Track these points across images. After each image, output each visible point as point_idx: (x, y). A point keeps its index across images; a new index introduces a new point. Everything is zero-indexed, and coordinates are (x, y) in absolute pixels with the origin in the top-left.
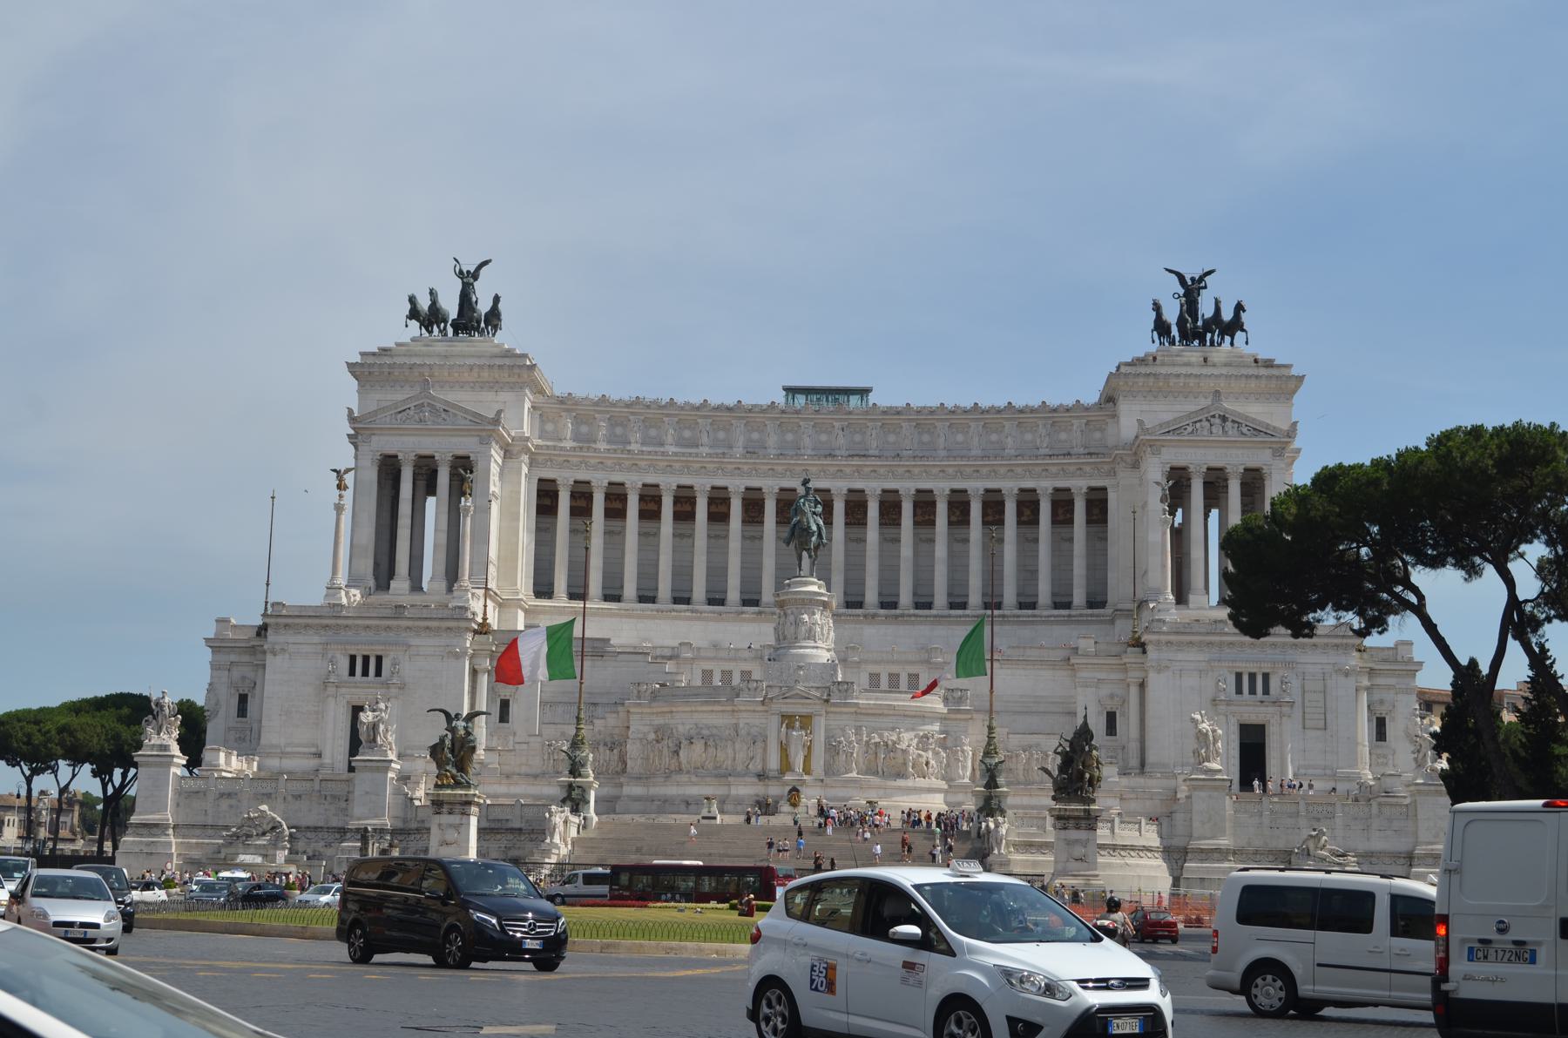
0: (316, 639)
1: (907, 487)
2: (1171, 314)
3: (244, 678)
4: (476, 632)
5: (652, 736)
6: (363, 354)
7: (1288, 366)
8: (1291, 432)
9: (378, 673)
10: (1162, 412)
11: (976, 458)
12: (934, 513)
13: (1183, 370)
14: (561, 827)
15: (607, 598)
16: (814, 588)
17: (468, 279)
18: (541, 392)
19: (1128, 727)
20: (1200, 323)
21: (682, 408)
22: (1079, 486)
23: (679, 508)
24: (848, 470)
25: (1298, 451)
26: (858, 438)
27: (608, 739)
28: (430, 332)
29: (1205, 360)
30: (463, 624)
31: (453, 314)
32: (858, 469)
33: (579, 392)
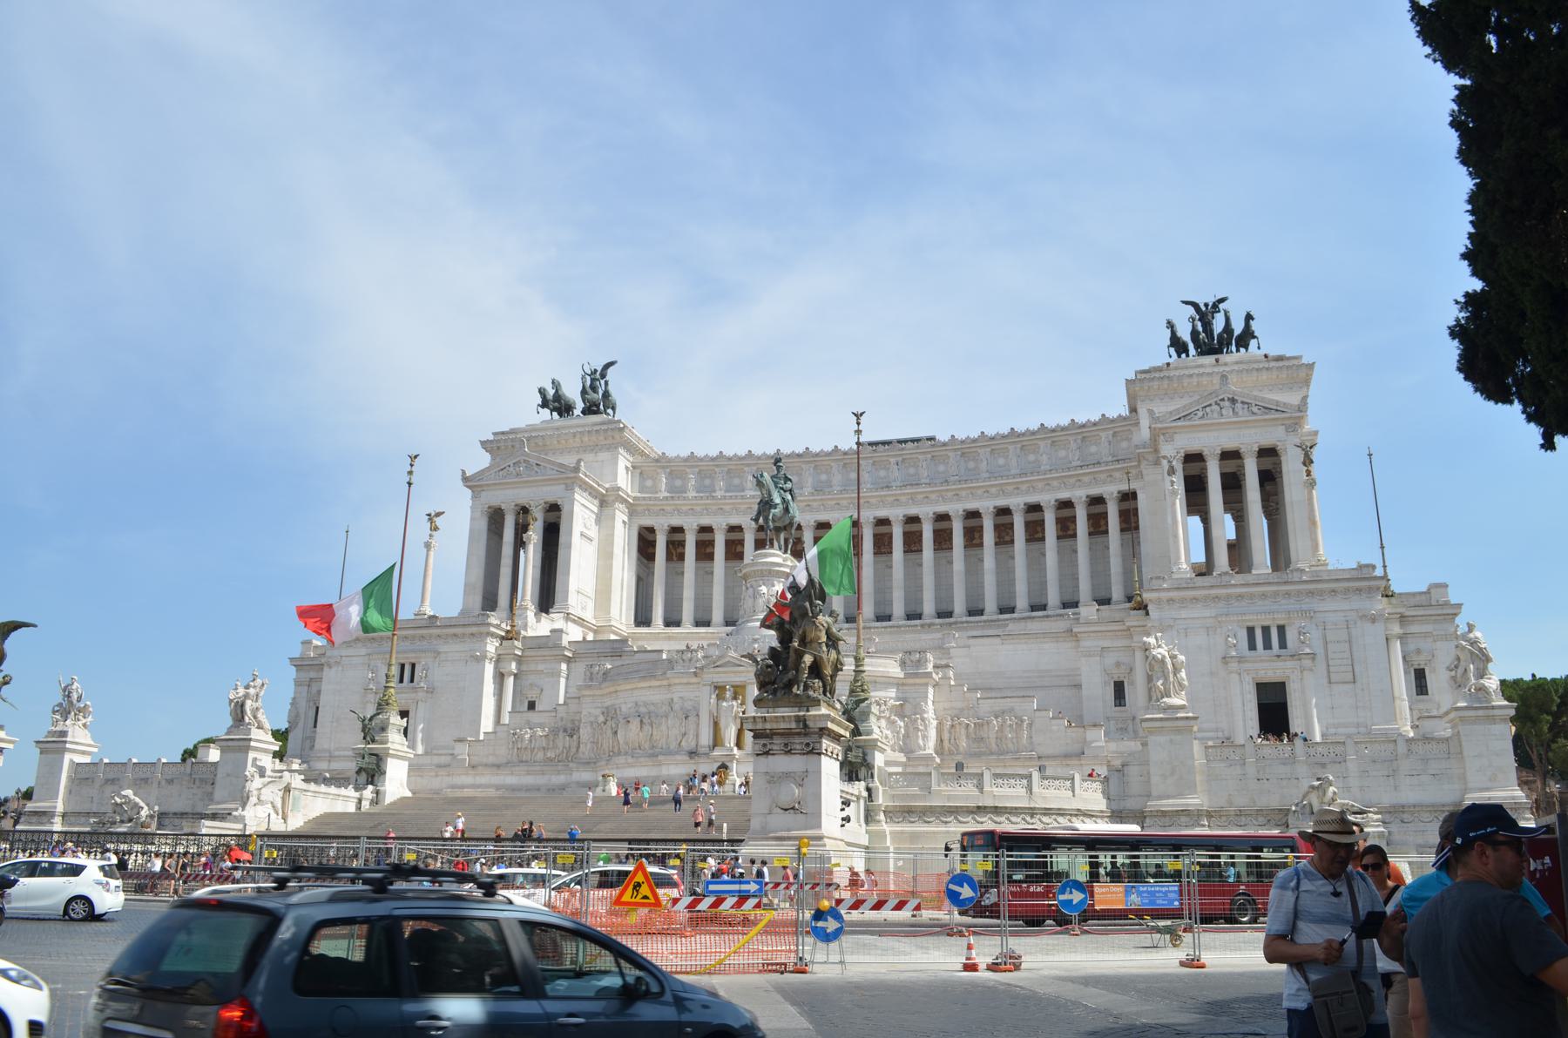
2: (1185, 334)
4: (503, 638)
5: (601, 719)
15: (698, 624)
21: (759, 458)
22: (1109, 491)
24: (903, 499)
25: (1316, 433)
26: (912, 471)
27: (569, 725)
30: (483, 629)
32: (912, 497)
33: (671, 453)
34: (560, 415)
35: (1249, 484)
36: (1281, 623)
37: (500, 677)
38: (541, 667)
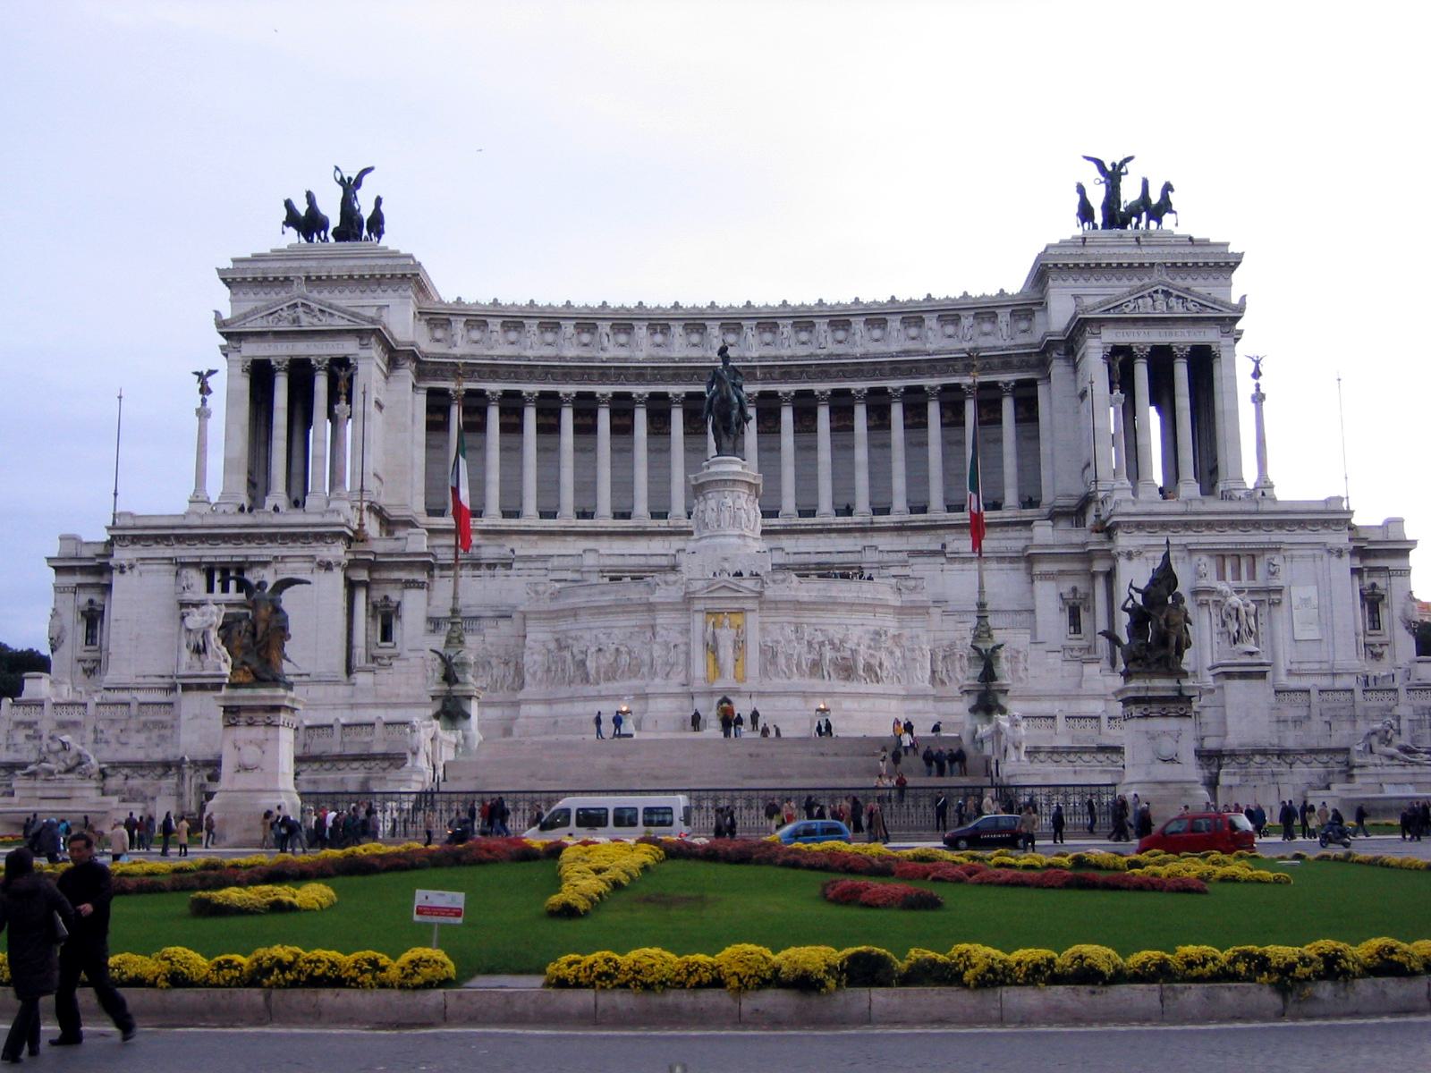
0: (169, 553)
3: (91, 602)
4: (350, 540)
5: (552, 646)
6: (235, 261)
7: (1226, 245)
8: (1240, 308)
10: (1097, 294)
11: (899, 354)
12: (852, 419)
13: (1112, 251)
14: (429, 748)
16: (738, 468)
17: (350, 187)
20: (1122, 210)
23: (580, 421)
25: (1240, 332)
28: (312, 241)
29: (1137, 239)
31: (335, 221)
37: (351, 586)
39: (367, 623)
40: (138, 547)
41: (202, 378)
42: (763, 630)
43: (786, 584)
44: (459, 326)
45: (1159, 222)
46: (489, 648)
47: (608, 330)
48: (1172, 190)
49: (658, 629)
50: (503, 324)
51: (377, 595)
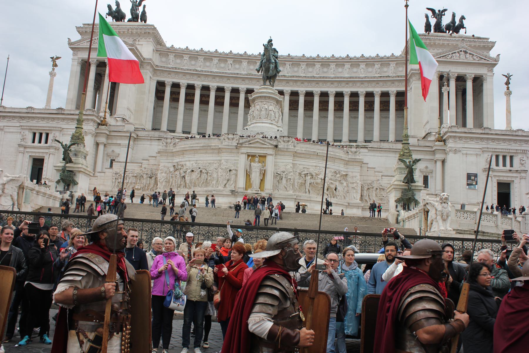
0: (18, 124)
1: (317, 90)
4: (99, 124)
5: (172, 169)
6: (84, 25)
7: (488, 39)
9: (46, 142)
12: (328, 106)
18: (161, 45)
19: (435, 183)
27: (149, 173)
31: (128, 16)
34: (116, 21)
35: (468, 91)
36: (512, 154)
38: (119, 142)
39: (103, 162)
40: (5, 121)
41: (54, 59)
42: (275, 165)
43: (290, 143)
44: (171, 57)
45: (457, 32)
46: (143, 169)
47: (231, 62)
48: (465, 19)
49: (223, 161)
50: (189, 58)
51: (110, 149)
